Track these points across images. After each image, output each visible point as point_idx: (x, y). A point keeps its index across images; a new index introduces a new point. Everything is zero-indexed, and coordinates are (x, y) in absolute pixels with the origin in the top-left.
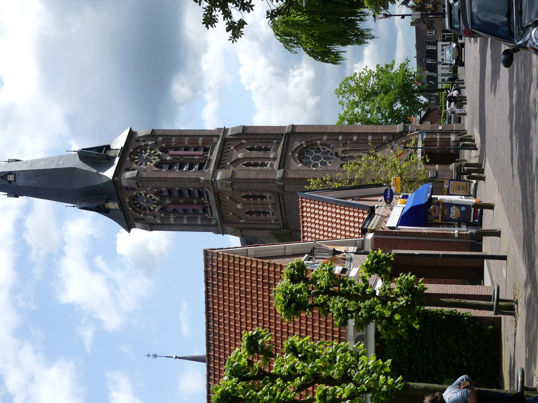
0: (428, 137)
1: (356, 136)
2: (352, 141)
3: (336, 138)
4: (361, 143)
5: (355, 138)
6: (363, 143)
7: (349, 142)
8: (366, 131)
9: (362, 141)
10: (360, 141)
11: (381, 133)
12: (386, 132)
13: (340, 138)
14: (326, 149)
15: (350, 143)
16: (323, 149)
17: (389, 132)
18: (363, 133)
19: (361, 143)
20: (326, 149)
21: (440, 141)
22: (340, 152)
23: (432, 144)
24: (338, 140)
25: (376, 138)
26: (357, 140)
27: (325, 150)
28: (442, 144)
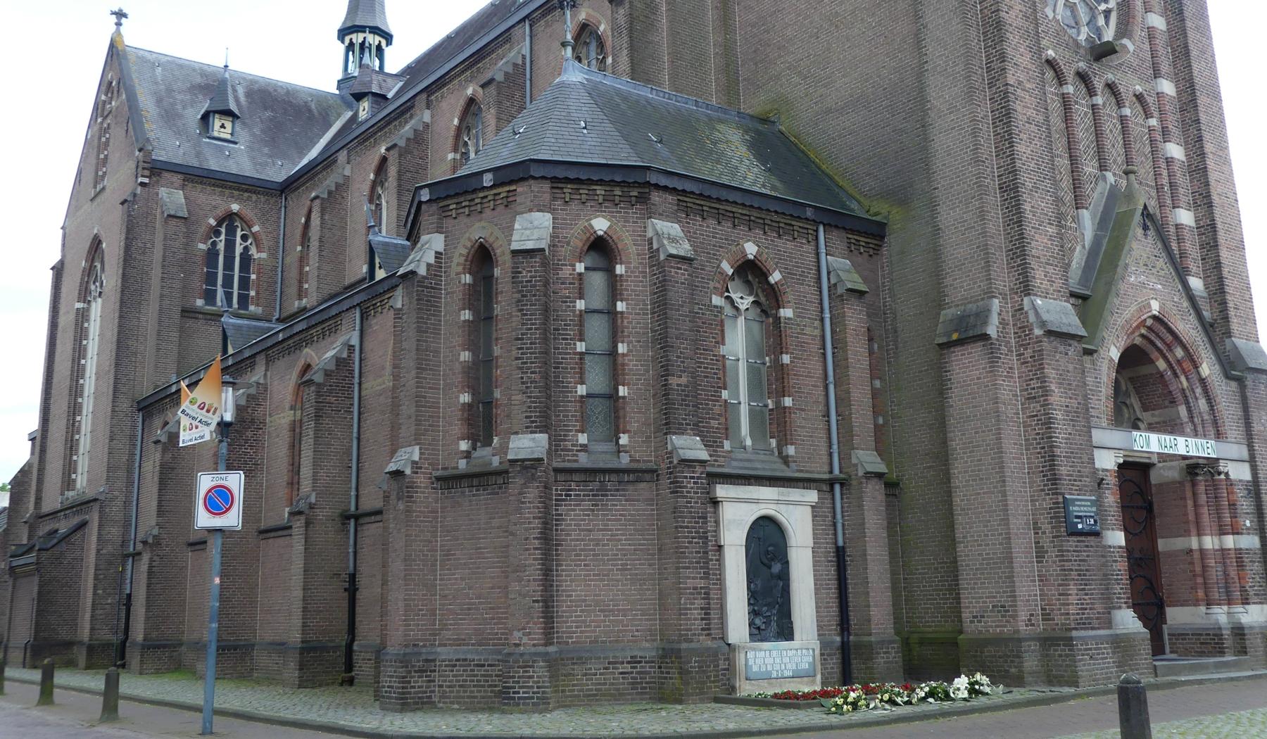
0: (1240, 493)
1: (1184, 159)
2: (1159, 138)
3: (1165, 67)
4: (1157, 175)
5: (1175, 150)
6: (1159, 188)
7: (1153, 122)
8: (1215, 197)
9: (1165, 180)
10: (1165, 173)
11: (1218, 265)
12: (1227, 289)
13: (1167, 87)
14: (1107, 23)
15: (1151, 130)
16: (1107, 13)
17: (1231, 305)
18: (1207, 184)
19: (1157, 175)
20: (1107, 23)
21: (1223, 551)
22: (1110, 77)
23: (1205, 510)
24: (1157, 74)
25: (1188, 245)
26: (1169, 161)
27: (1101, 21)
28: (1212, 562)
